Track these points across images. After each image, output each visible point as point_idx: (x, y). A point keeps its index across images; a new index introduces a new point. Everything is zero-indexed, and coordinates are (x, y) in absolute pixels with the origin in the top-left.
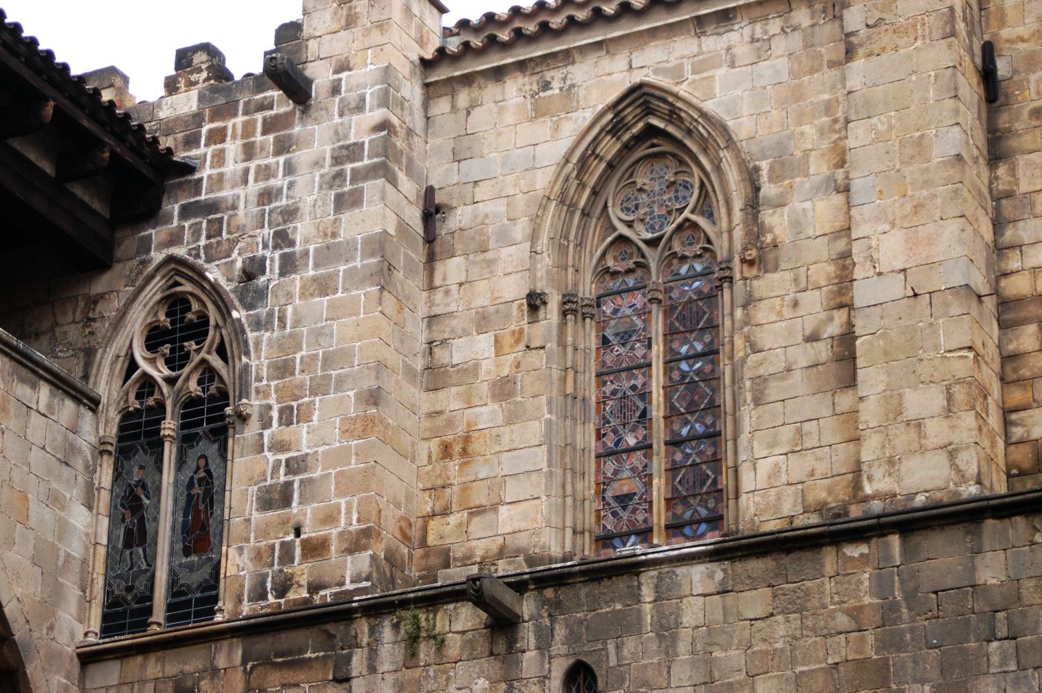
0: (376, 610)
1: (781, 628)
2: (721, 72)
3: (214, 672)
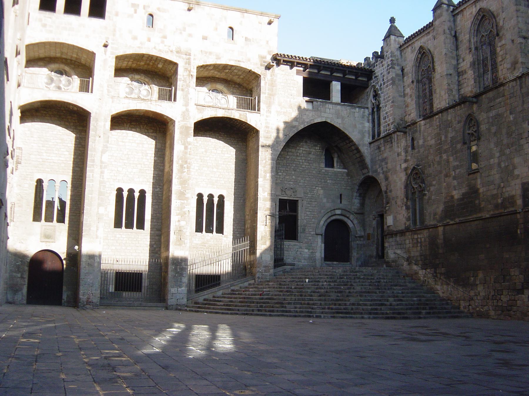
0: (394, 132)
1: (430, 129)
2: (429, 41)
3: (381, 144)
